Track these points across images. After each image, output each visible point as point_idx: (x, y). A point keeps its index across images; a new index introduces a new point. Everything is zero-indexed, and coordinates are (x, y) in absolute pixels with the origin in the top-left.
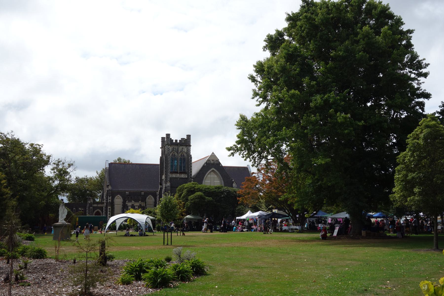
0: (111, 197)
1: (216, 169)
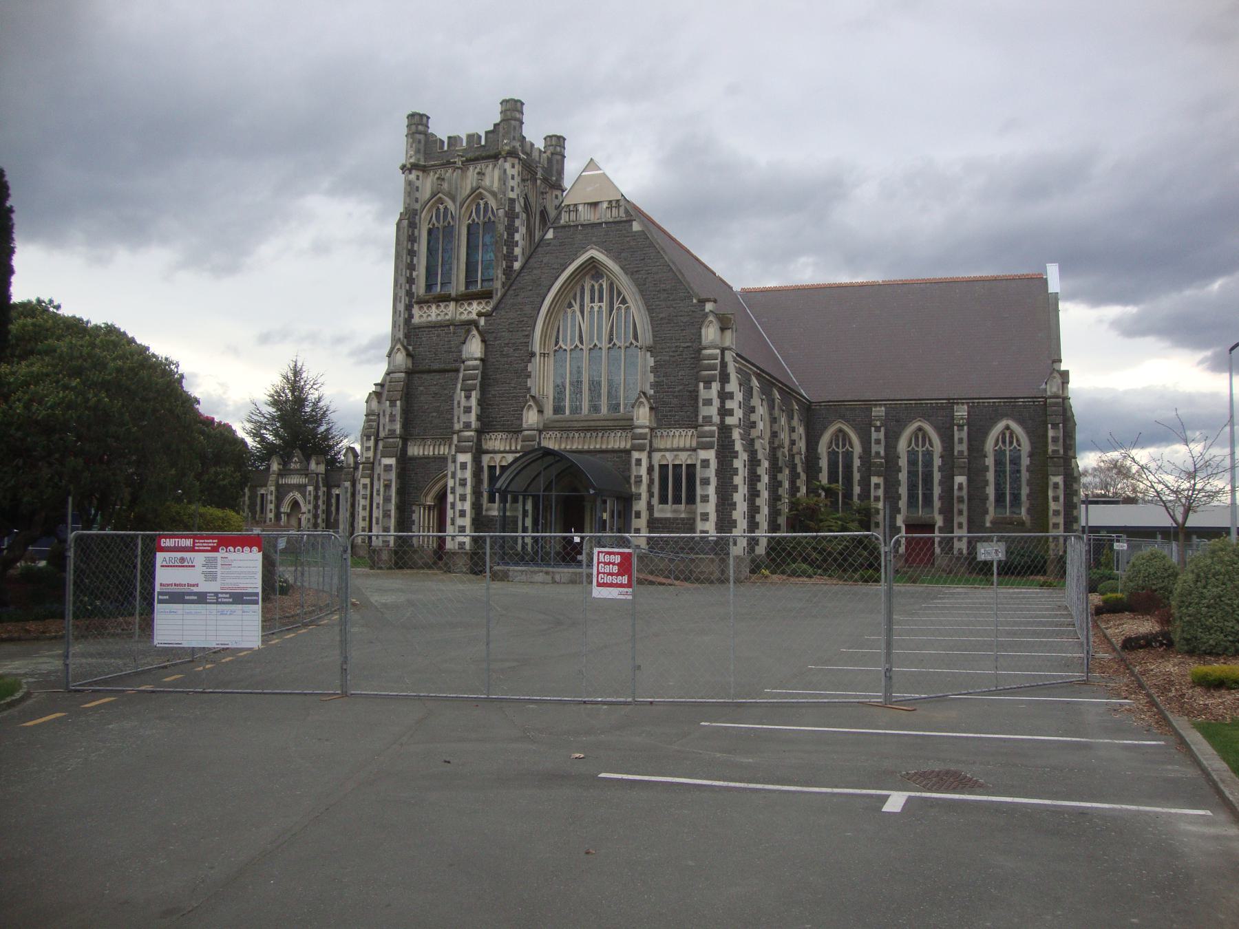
1: (608, 252)
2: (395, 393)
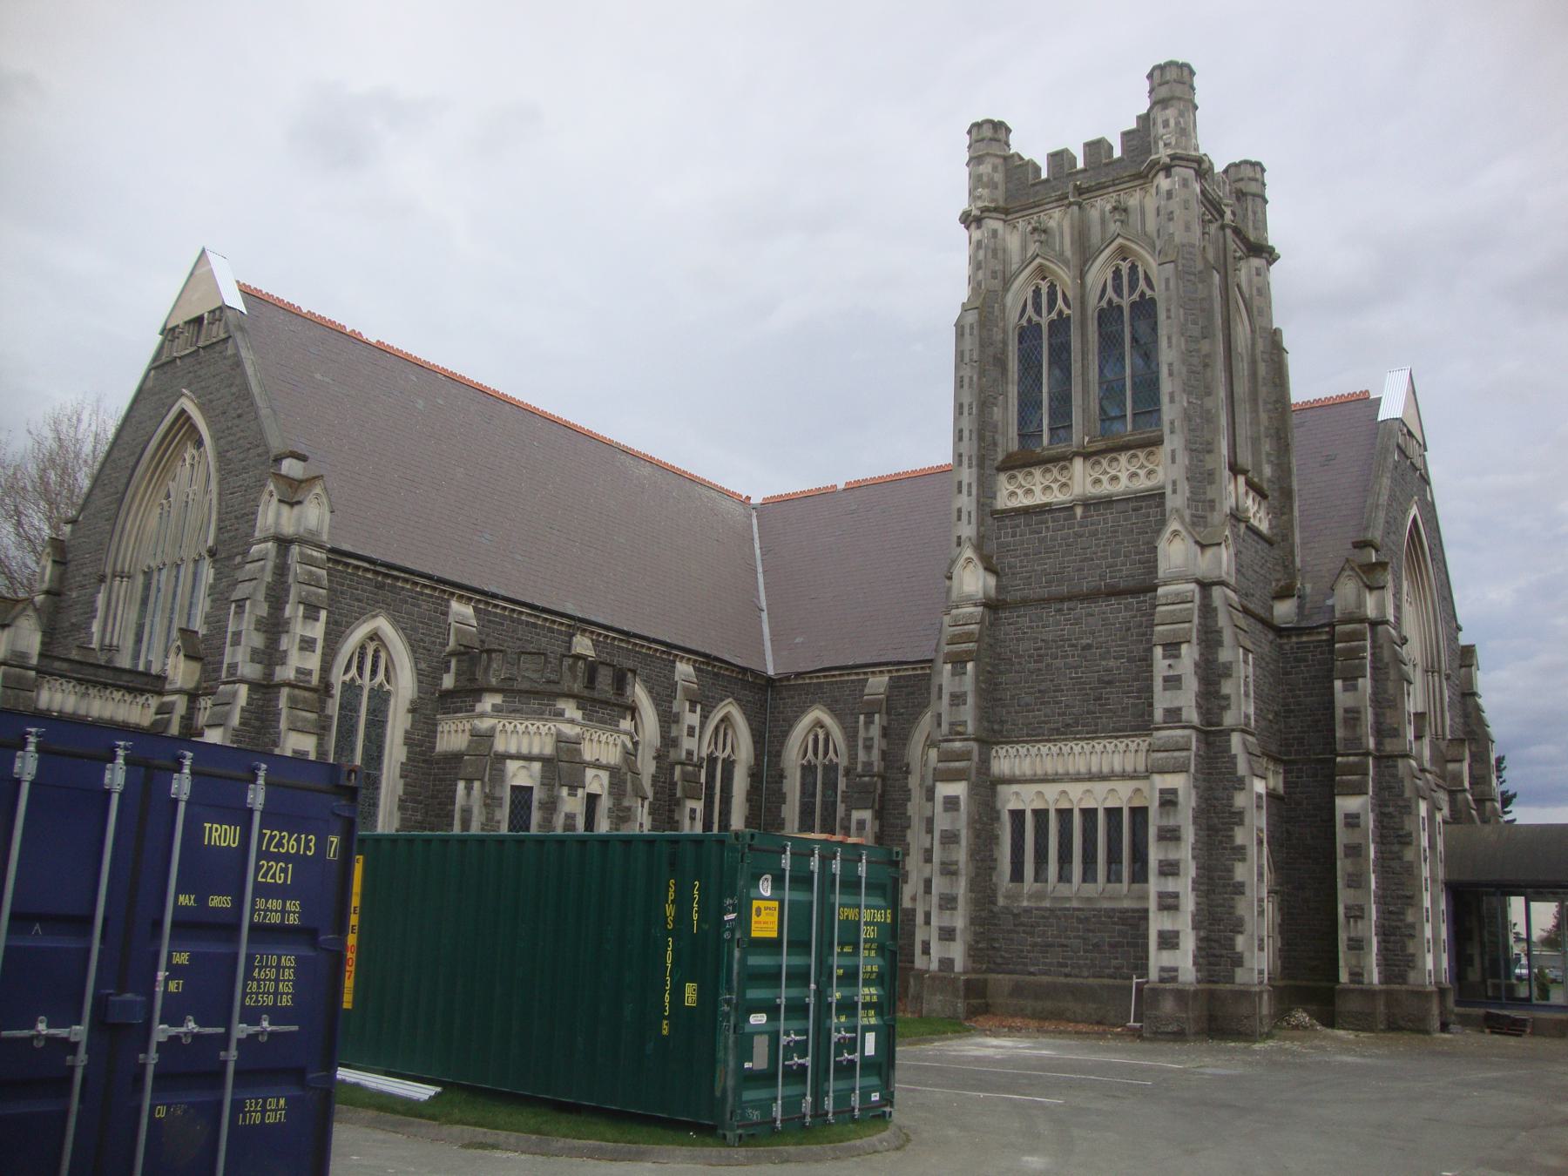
0: (323, 615)
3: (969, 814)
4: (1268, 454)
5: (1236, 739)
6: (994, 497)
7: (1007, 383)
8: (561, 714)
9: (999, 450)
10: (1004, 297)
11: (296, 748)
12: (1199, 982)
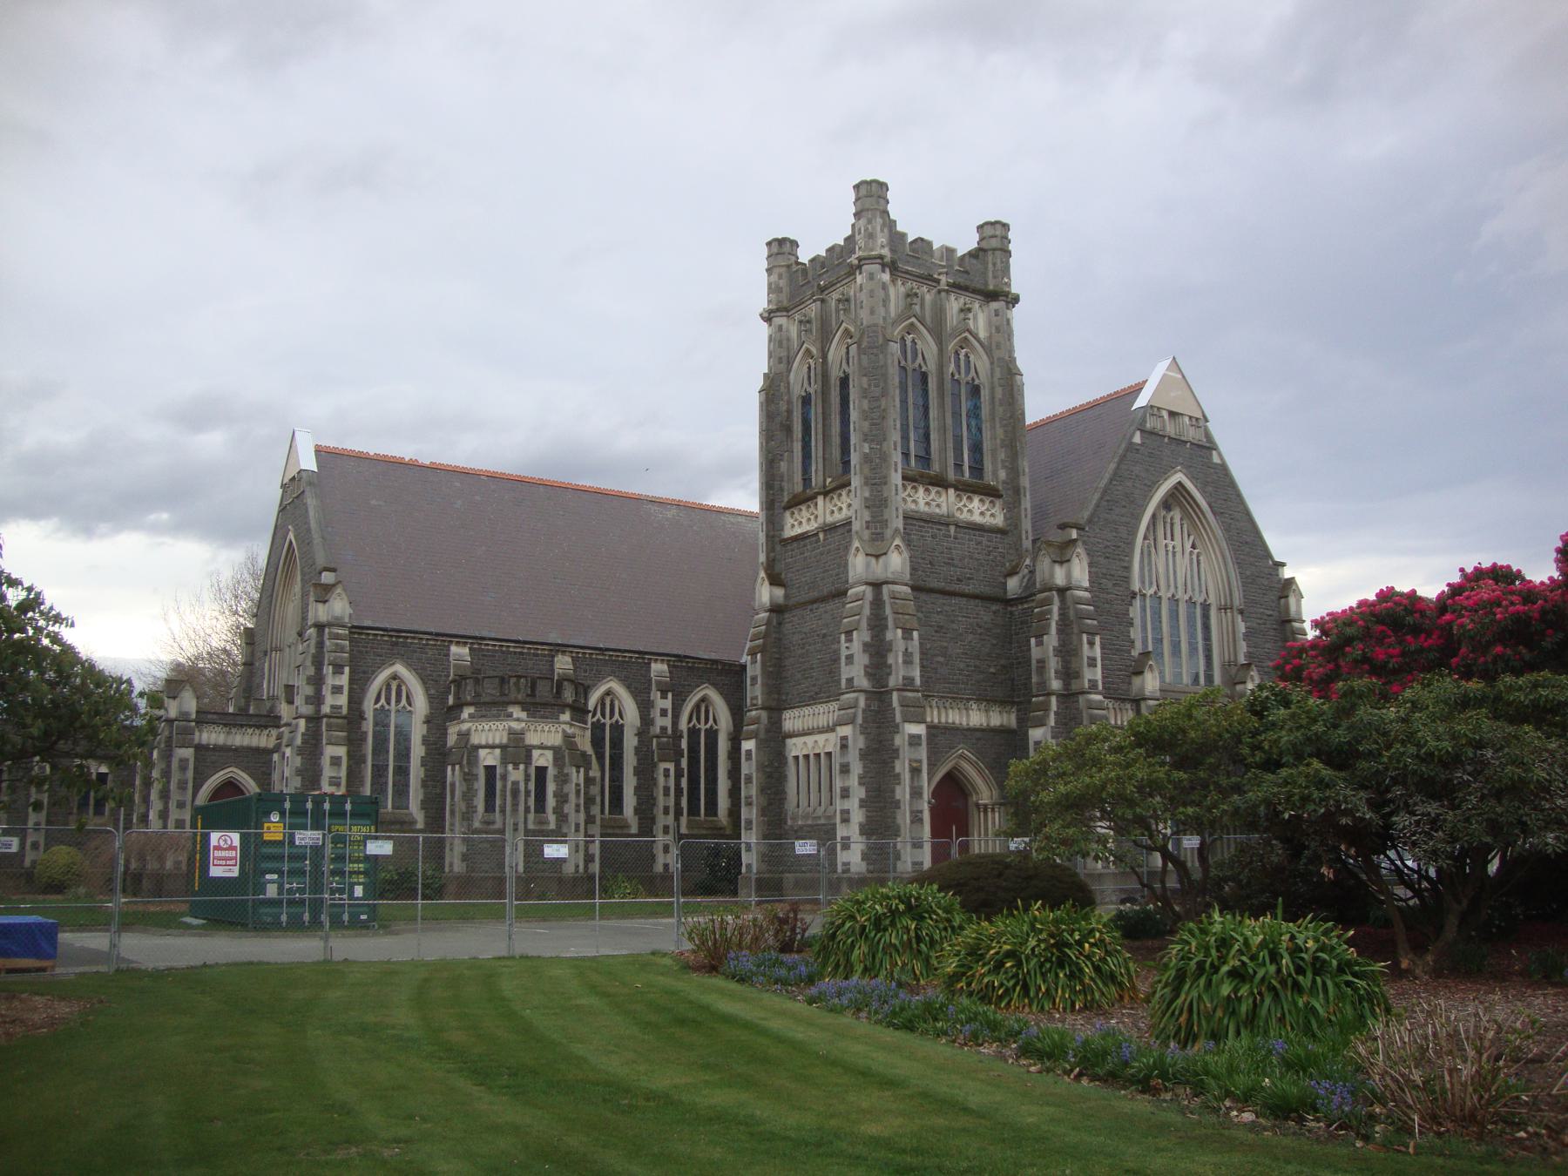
0: (347, 670)
1: (1192, 478)
2: (907, 617)
3: (757, 761)
4: (1002, 461)
5: (895, 695)
6: (782, 530)
7: (792, 442)
8: (510, 715)
9: (786, 493)
10: (788, 376)
11: (333, 755)
12: (869, 871)
